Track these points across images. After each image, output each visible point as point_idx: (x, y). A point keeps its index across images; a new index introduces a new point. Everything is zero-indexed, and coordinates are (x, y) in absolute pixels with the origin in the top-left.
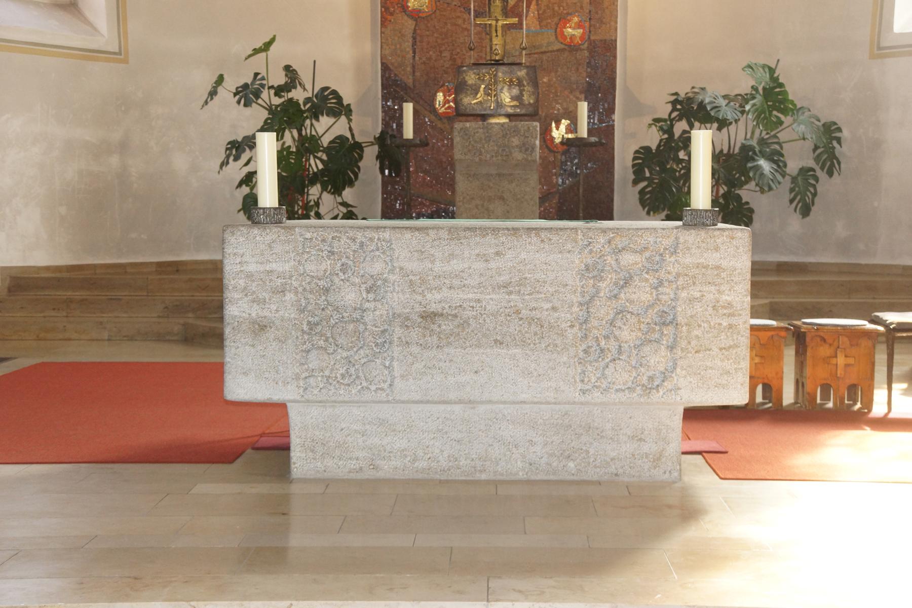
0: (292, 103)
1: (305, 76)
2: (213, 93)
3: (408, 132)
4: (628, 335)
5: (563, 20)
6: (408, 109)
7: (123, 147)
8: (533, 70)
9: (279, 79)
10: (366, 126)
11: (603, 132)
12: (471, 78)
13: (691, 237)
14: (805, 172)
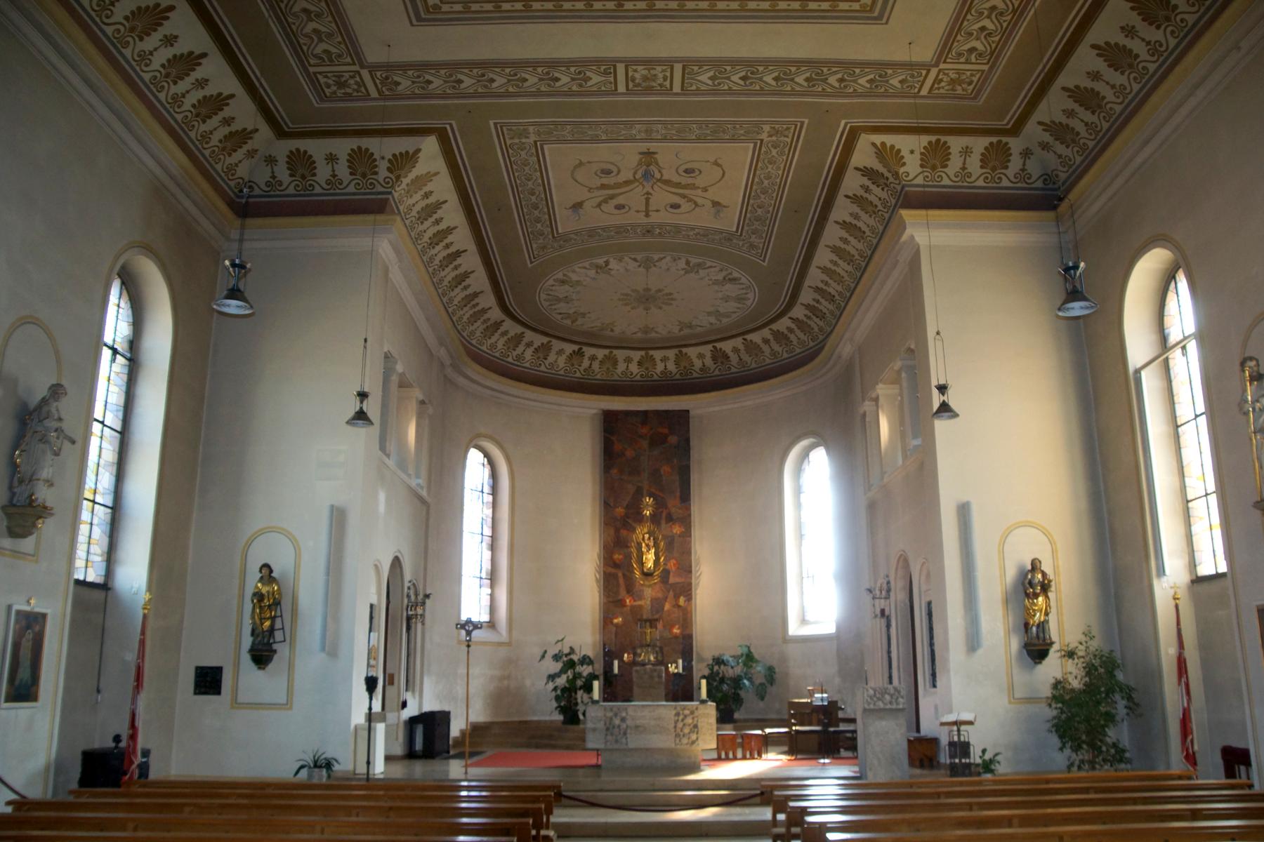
0: (571, 660)
1: (577, 651)
2: (543, 657)
3: (616, 671)
4: (686, 730)
5: (673, 626)
6: (616, 663)
7: (509, 677)
8: (661, 648)
9: (566, 651)
10: (599, 668)
11: (688, 667)
12: (639, 651)
13: (701, 707)
14: (761, 684)
